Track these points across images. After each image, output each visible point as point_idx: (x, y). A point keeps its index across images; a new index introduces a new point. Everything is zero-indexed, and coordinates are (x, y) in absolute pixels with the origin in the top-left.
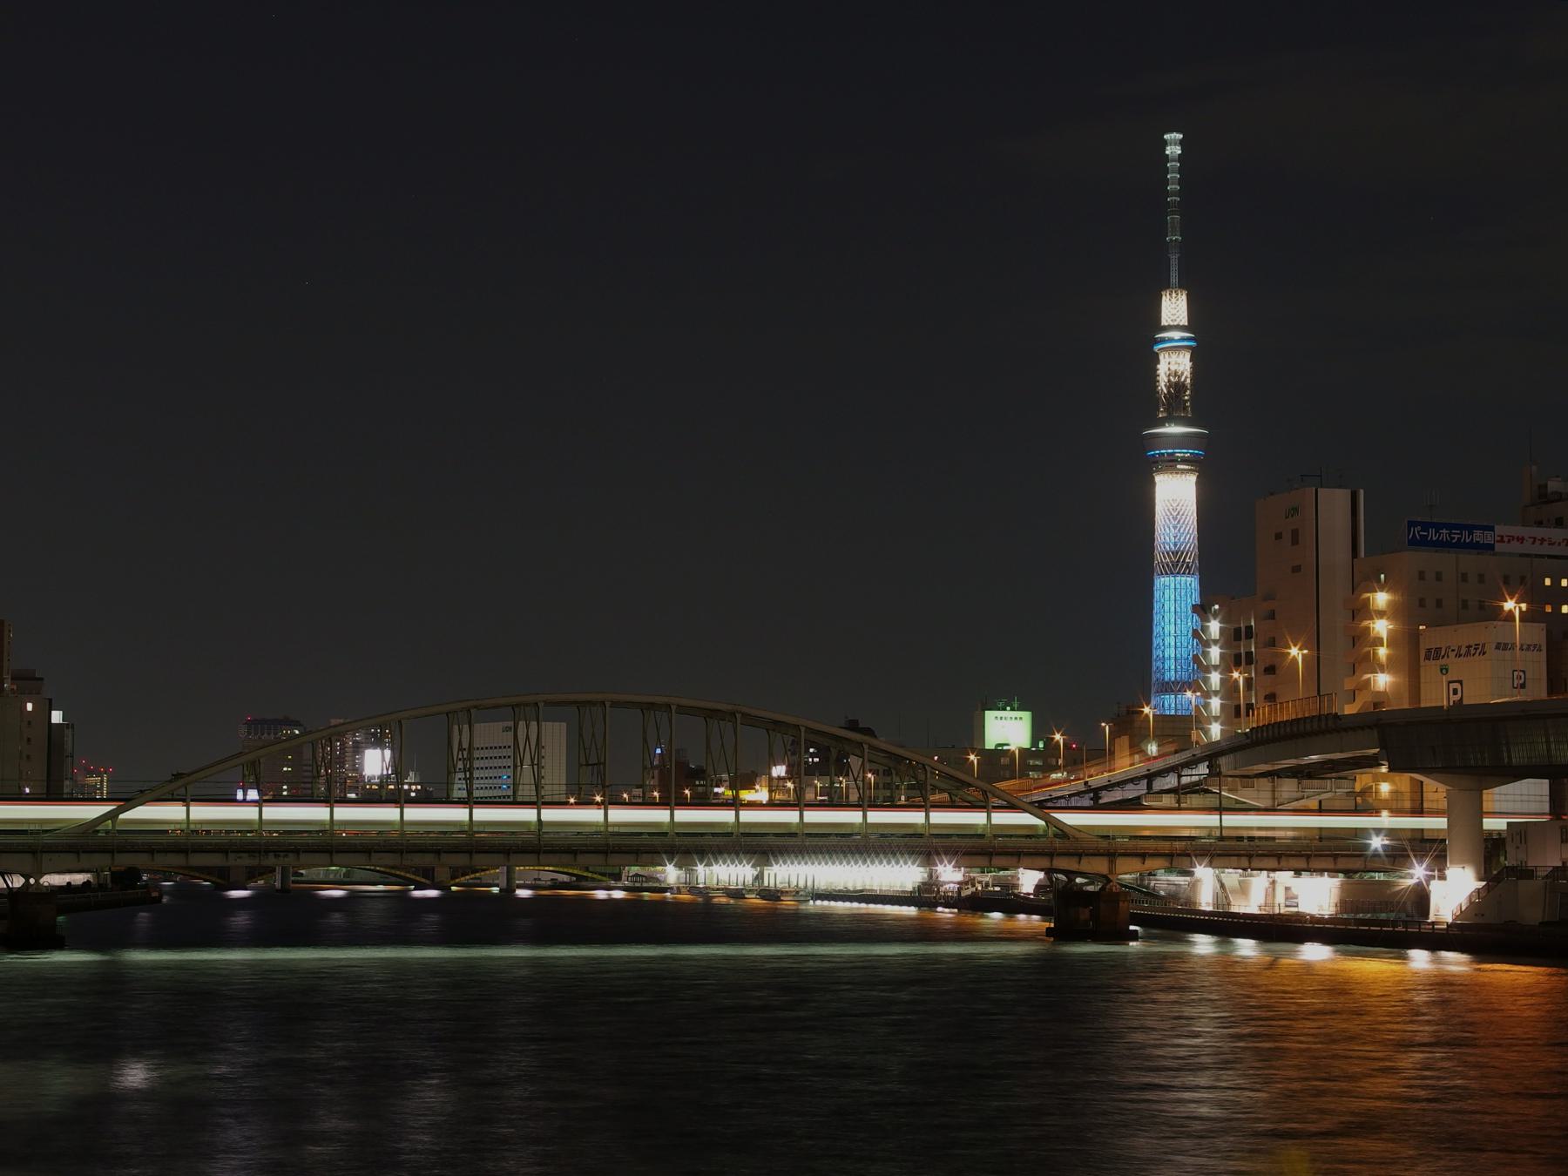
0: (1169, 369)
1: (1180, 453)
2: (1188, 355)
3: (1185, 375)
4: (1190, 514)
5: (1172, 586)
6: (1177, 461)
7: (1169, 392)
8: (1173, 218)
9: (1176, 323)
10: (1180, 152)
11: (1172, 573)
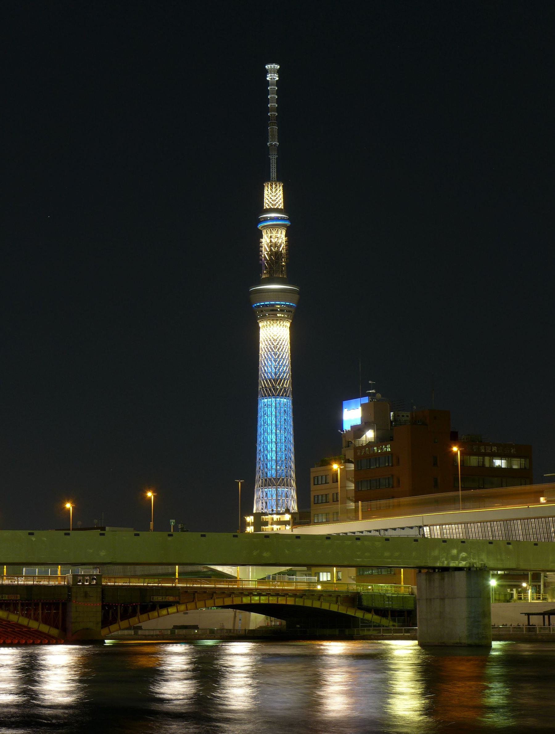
0: (271, 241)
1: (279, 304)
2: (284, 233)
3: (282, 246)
4: (286, 351)
5: (274, 404)
6: (277, 310)
7: (271, 259)
8: (273, 129)
9: (276, 207)
10: (277, 79)
11: (273, 395)
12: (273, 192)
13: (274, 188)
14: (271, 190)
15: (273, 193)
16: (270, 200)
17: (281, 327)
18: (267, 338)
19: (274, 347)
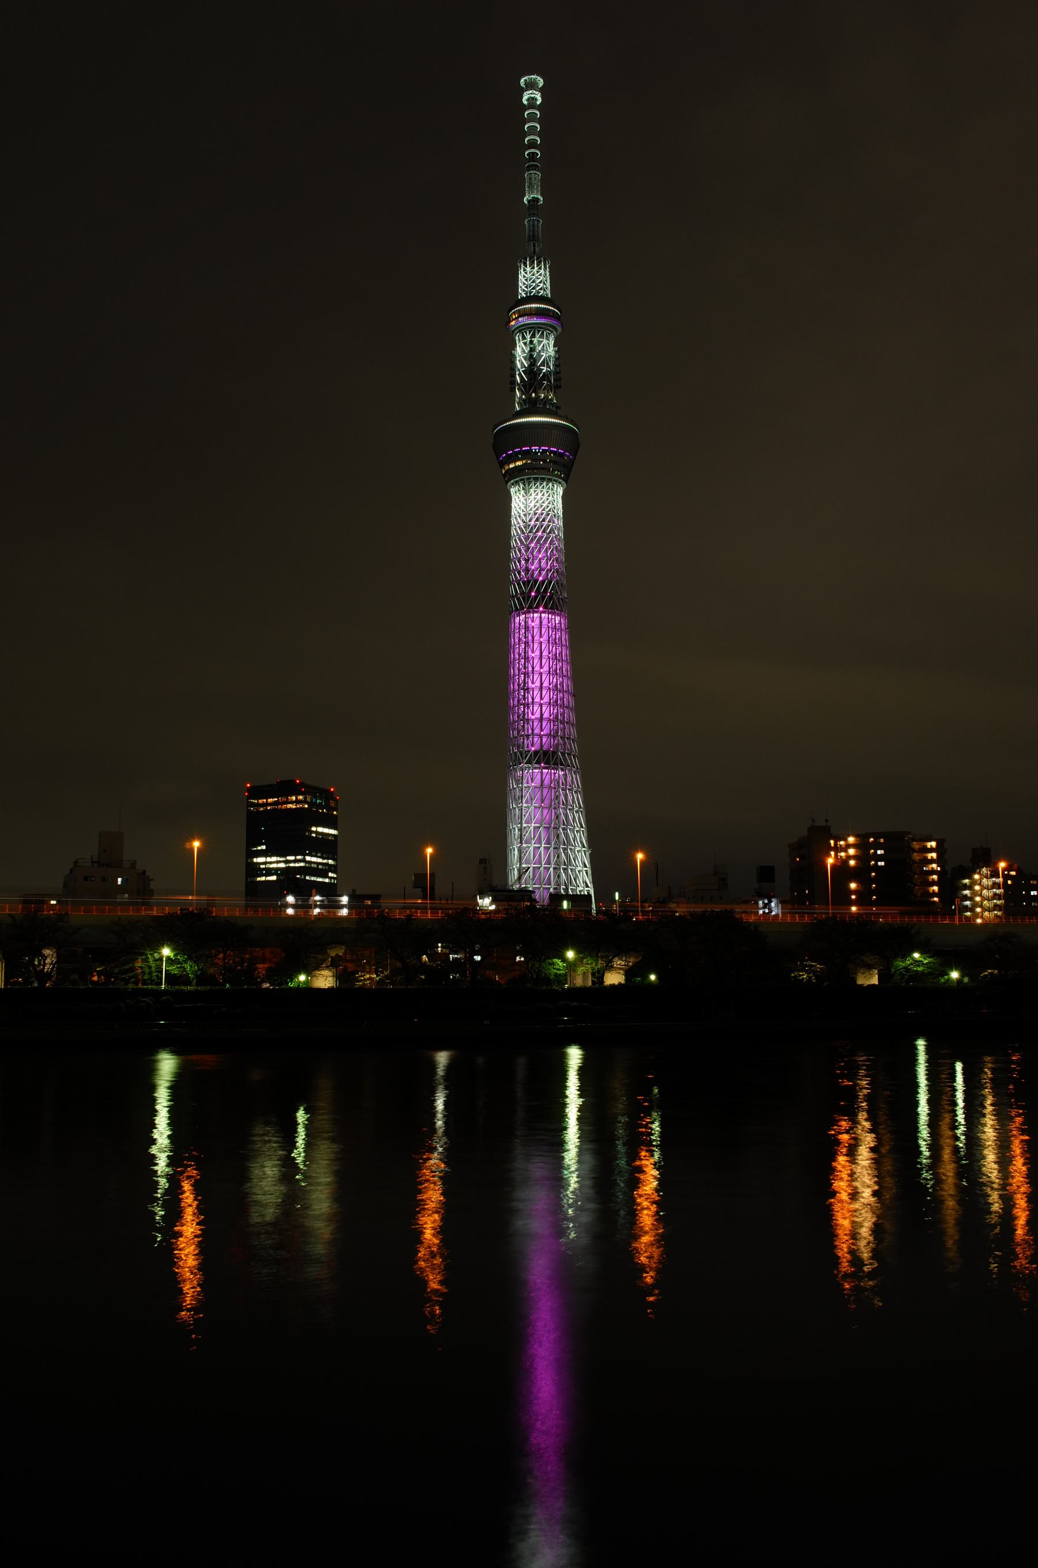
9: (532, 295)
12: (526, 273)
13: (528, 266)
14: (524, 270)
15: (526, 273)
16: (523, 287)
17: (538, 490)
18: (516, 513)
19: (525, 527)
